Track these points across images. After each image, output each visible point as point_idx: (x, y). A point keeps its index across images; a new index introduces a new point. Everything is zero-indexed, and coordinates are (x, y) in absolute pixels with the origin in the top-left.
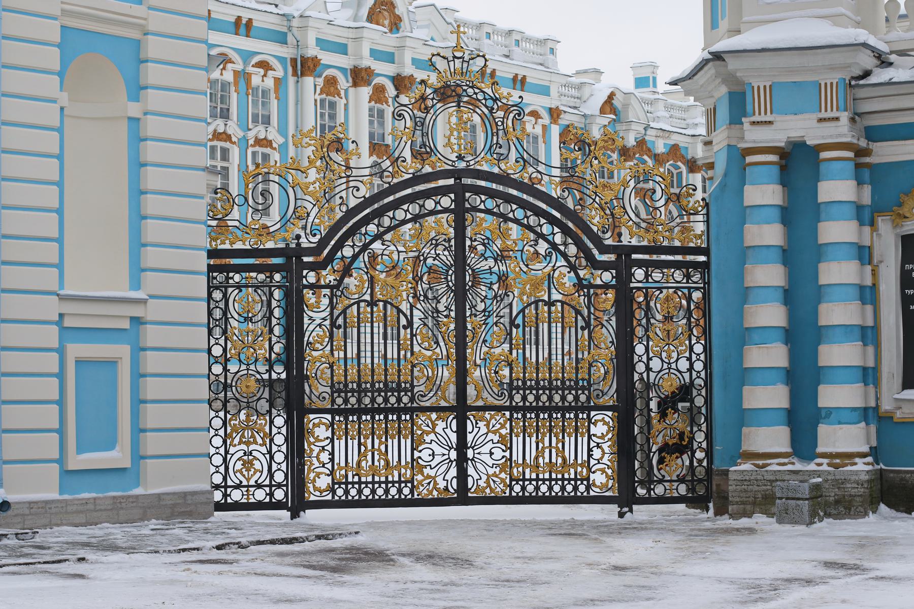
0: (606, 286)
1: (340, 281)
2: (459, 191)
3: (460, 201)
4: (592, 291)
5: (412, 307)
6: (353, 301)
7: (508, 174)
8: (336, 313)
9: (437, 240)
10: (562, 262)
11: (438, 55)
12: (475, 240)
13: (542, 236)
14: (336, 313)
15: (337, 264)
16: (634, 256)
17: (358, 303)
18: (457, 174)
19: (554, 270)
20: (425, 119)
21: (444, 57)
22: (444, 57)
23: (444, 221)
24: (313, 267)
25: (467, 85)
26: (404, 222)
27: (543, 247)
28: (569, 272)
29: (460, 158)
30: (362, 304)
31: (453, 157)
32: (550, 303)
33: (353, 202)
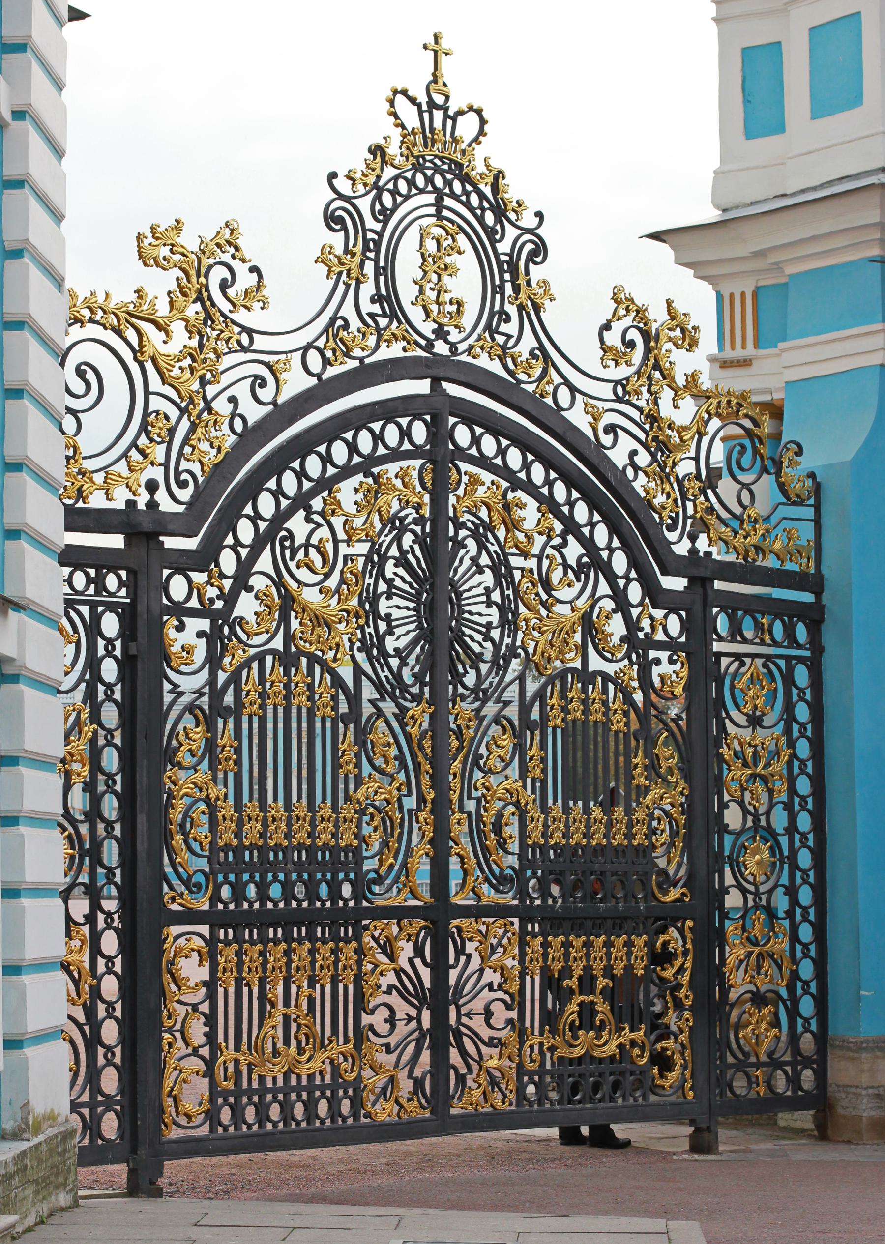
0: (671, 645)
1: (231, 600)
2: (436, 411)
3: (438, 433)
4: (653, 654)
5: (358, 671)
6: (252, 651)
7: (519, 382)
8: (222, 677)
9: (402, 520)
10: (604, 588)
11: (404, 93)
12: (463, 526)
13: (571, 527)
14: (222, 677)
15: (228, 562)
16: (718, 585)
17: (260, 658)
18: (436, 369)
19: (592, 607)
20: (380, 235)
21: (413, 101)
22: (413, 101)
23: (415, 474)
24: (183, 563)
25: (450, 171)
26: (346, 472)
27: (574, 550)
28: (614, 611)
29: (441, 333)
30: (269, 659)
31: (428, 328)
32: (586, 677)
33: (254, 413)
